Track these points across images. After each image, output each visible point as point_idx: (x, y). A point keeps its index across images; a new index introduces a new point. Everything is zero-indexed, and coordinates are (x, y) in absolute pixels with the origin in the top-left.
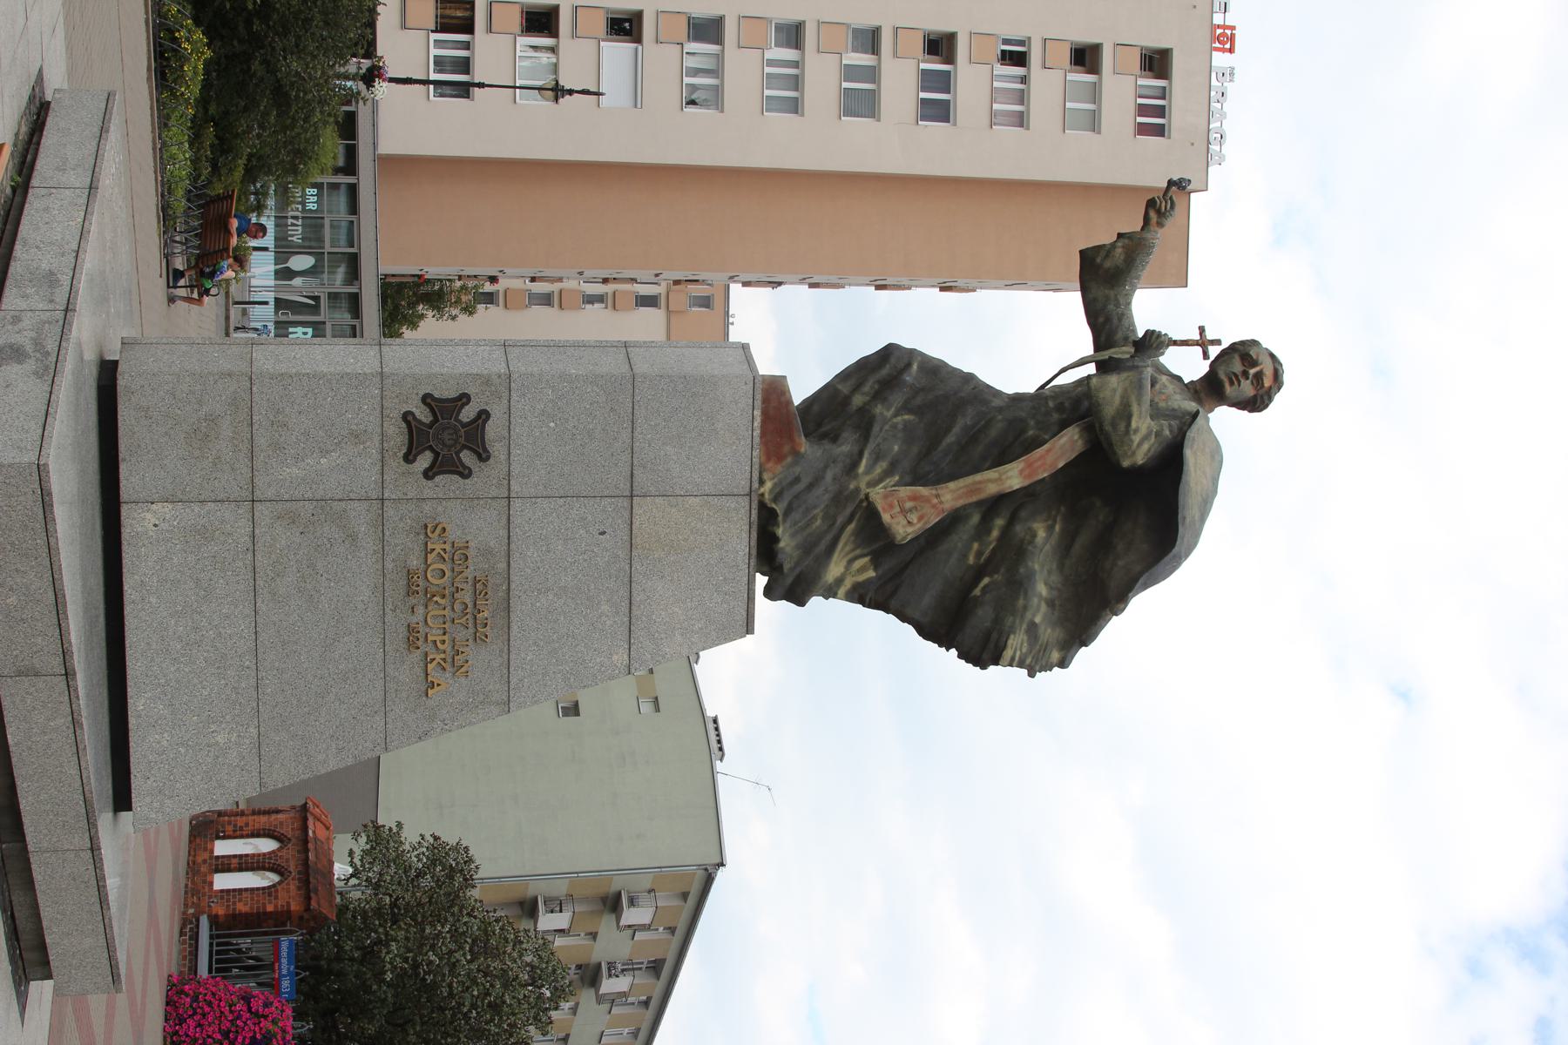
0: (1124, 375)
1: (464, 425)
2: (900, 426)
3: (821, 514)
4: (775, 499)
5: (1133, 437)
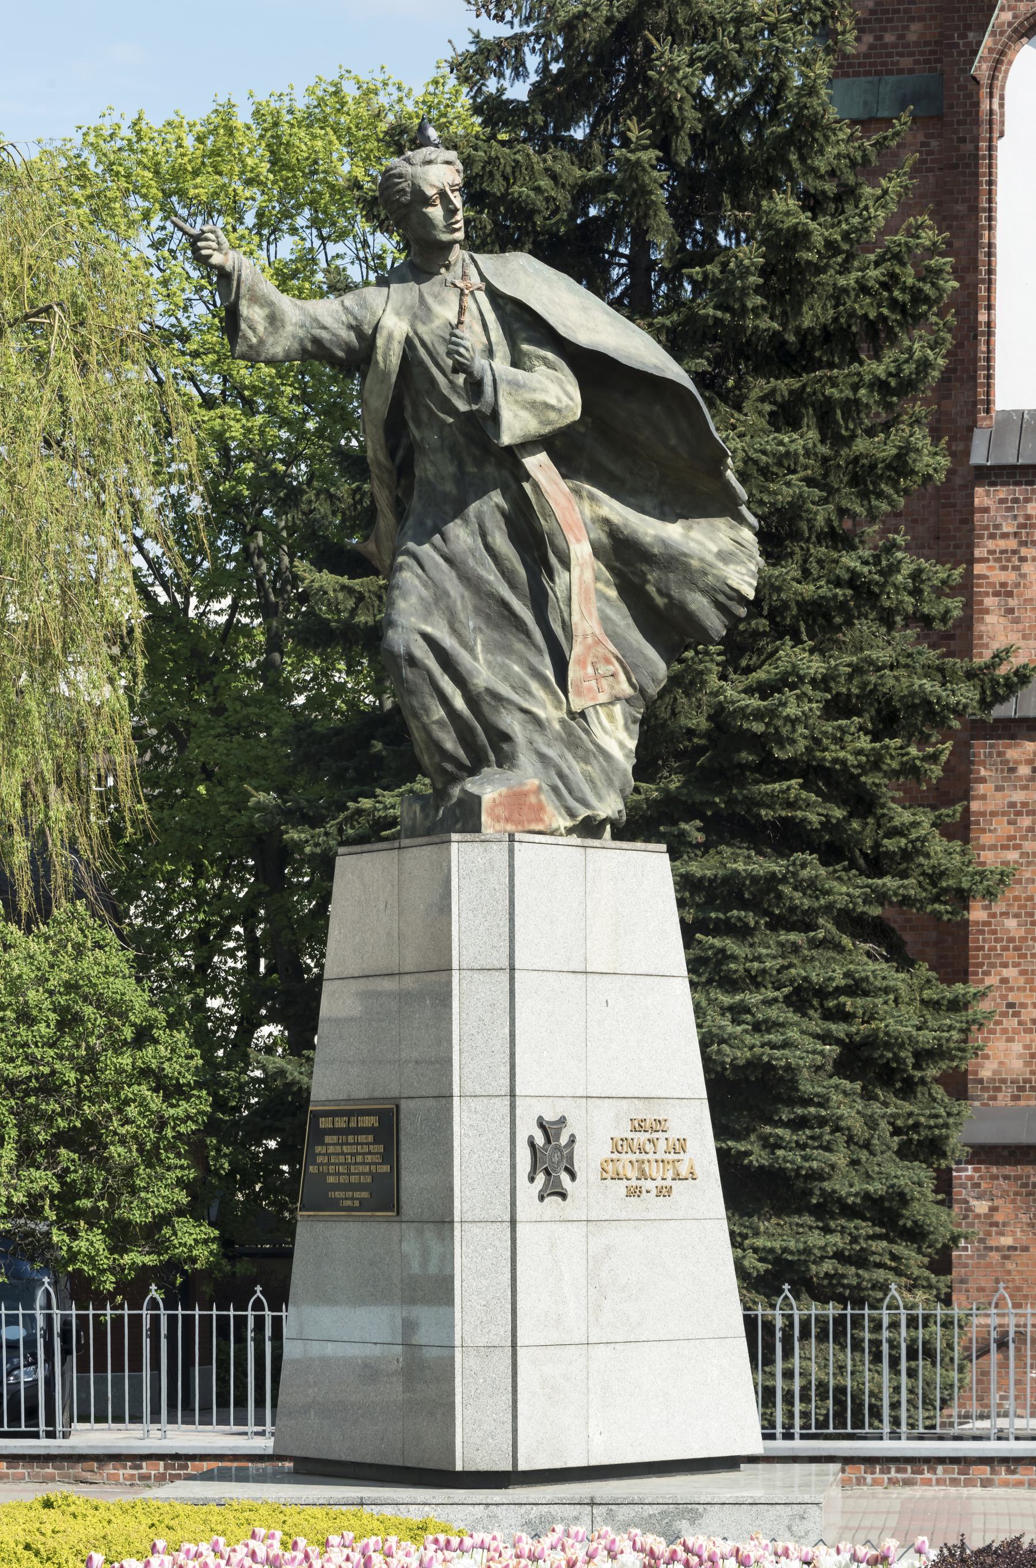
0: (502, 401)
1: (548, 1140)
2: (490, 657)
3: (582, 765)
4: (572, 815)
5: (564, 404)
